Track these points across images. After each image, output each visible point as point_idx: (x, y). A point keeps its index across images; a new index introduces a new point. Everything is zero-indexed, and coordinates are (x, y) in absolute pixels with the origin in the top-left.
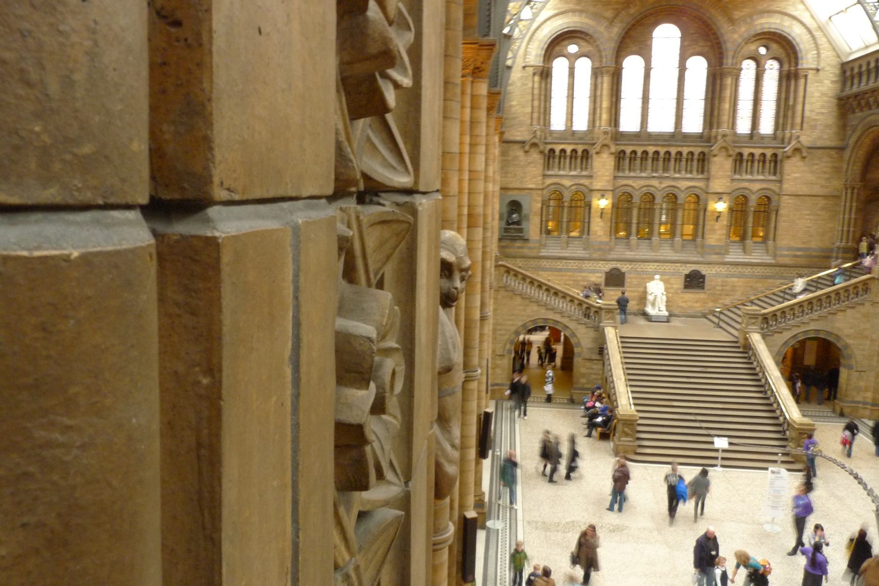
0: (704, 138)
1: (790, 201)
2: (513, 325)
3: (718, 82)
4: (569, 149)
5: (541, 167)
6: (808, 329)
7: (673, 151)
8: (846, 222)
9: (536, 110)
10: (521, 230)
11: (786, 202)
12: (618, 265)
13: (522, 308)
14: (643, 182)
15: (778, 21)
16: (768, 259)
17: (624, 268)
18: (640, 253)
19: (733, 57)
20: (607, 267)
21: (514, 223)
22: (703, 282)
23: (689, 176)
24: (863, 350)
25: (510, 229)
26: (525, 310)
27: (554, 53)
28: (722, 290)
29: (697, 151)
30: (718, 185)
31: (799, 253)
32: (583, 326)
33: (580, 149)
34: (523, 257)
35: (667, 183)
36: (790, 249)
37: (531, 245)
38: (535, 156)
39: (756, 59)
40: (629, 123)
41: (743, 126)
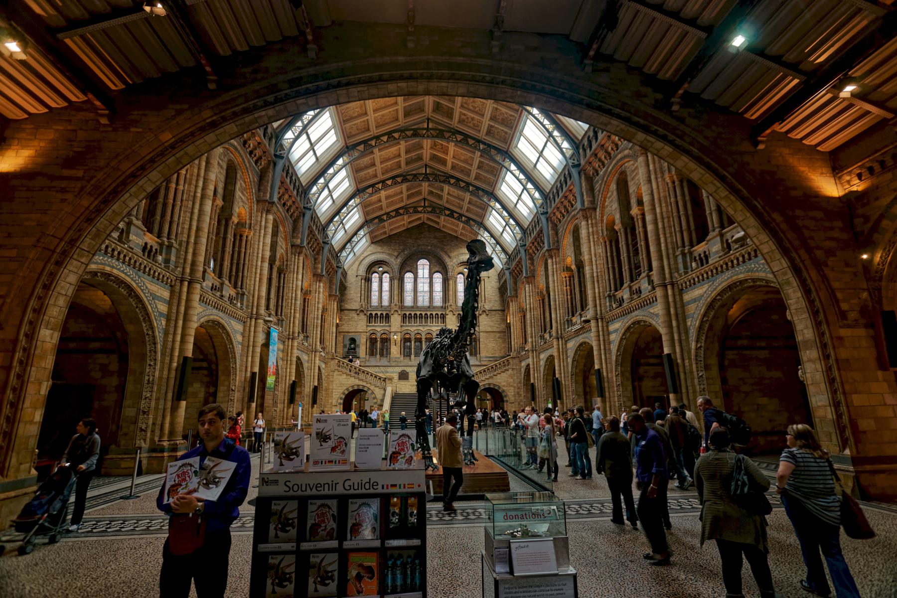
0: (444, 308)
4: (379, 313)
5: (365, 321)
7: (429, 313)
9: (363, 295)
10: (356, 353)
12: (405, 369)
14: (415, 328)
16: (478, 363)
20: (399, 369)
21: (352, 349)
27: (372, 271)
29: (439, 313)
33: (384, 313)
36: (486, 357)
38: (362, 316)
40: (408, 300)
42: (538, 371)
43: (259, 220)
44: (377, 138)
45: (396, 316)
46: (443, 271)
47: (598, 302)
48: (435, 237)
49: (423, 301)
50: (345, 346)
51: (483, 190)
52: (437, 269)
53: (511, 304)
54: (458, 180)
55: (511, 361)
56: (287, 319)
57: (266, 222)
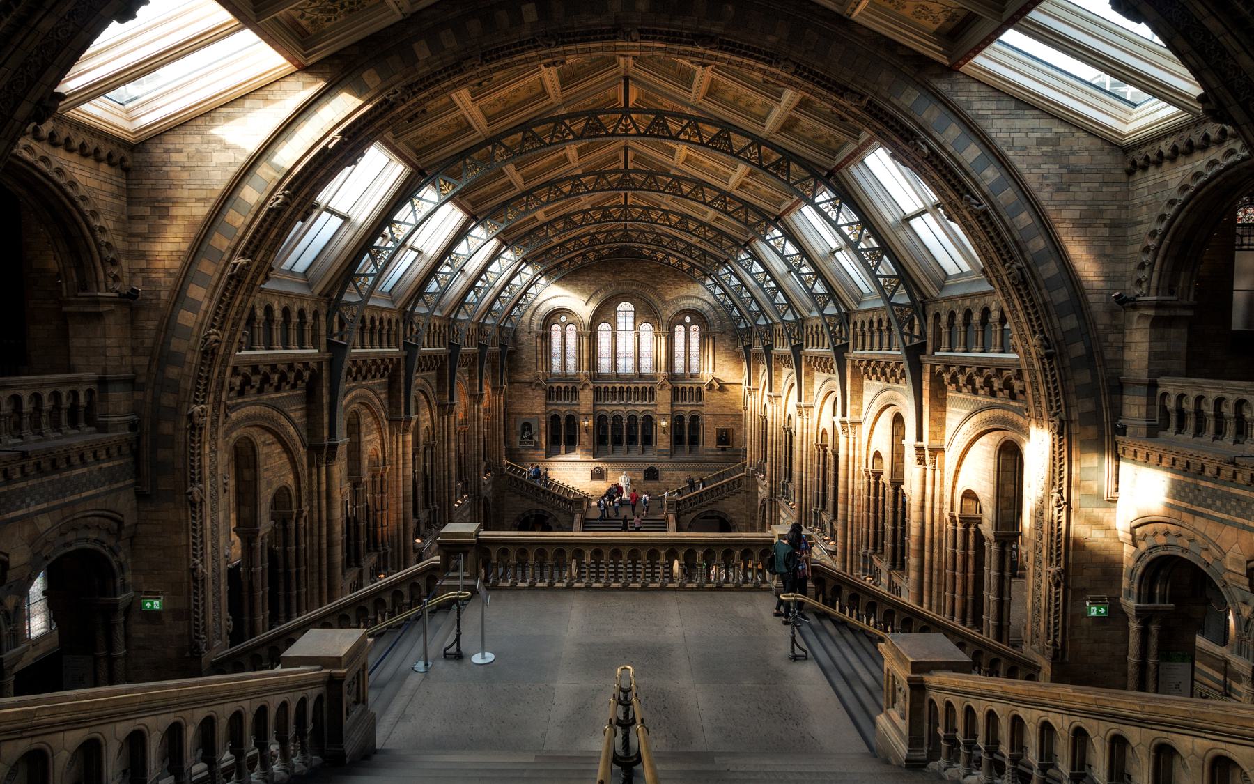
4: (563, 386)
7: (632, 386)
14: (613, 408)
29: (648, 386)
35: (629, 408)
36: (712, 451)
37: (540, 452)
39: (684, 323)
40: (604, 364)
43: (394, 447)
44: (549, 224)
45: (587, 391)
47: (848, 558)
49: (626, 365)
51: (713, 256)
53: (749, 398)
54: (676, 239)
55: (744, 480)
56: (439, 505)
57: (404, 447)
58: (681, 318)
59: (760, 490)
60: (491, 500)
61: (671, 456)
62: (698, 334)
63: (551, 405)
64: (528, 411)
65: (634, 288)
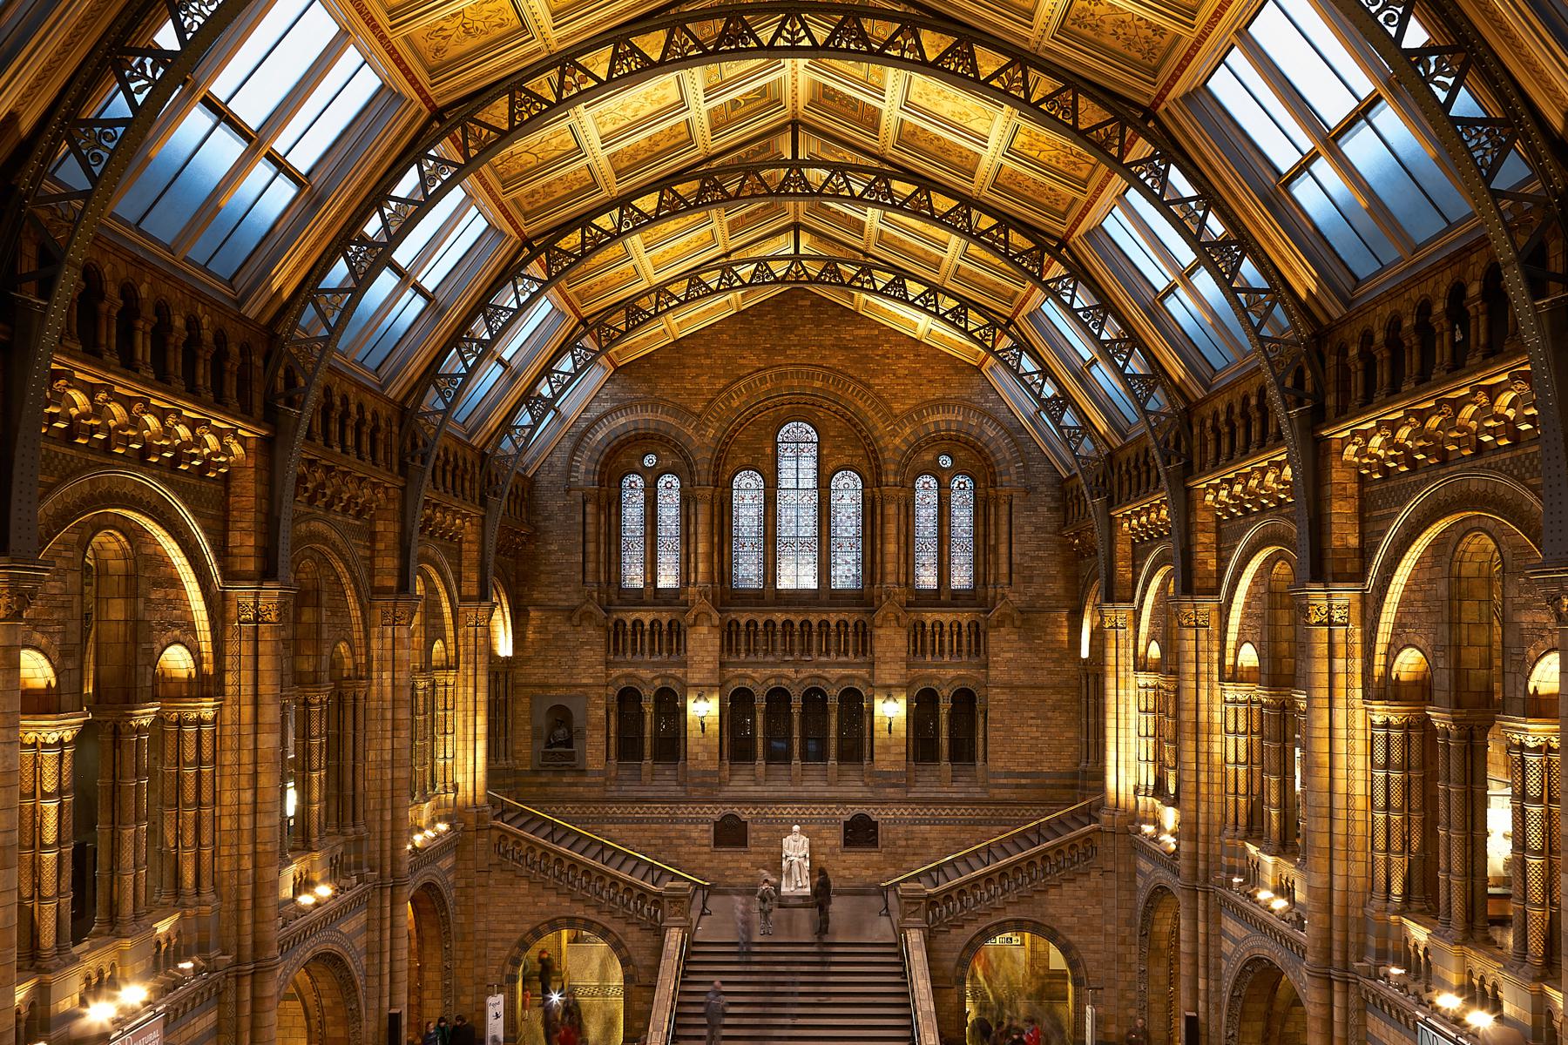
0: (863, 599)
1: (1004, 697)
2: (515, 931)
3: (879, 511)
5: (600, 650)
6: (1003, 919)
7: (814, 619)
8: (1091, 729)
10: (571, 756)
11: (996, 697)
13: (530, 899)
14: (768, 672)
15: (960, 418)
16: (976, 792)
17: (746, 813)
18: (771, 789)
19: (896, 475)
20: (716, 813)
21: (559, 744)
22: (876, 833)
23: (843, 659)
24: (1096, 952)
25: (554, 753)
26: (535, 904)
28: (907, 846)
29: (852, 618)
30: (888, 672)
31: (1023, 781)
32: (636, 928)
33: (665, 618)
34: (577, 801)
35: (806, 672)
36: (1009, 774)
37: (587, 780)
40: (748, 571)
41: (927, 578)
42: (1213, 972)
45: (704, 630)
46: (865, 464)
48: (840, 346)
49: (797, 574)
50: (535, 735)
52: (845, 460)
58: (929, 457)
59: (1144, 865)
60: (450, 896)
61: (907, 787)
62: (969, 495)
63: (617, 665)
64: (561, 681)
65: (818, 384)
